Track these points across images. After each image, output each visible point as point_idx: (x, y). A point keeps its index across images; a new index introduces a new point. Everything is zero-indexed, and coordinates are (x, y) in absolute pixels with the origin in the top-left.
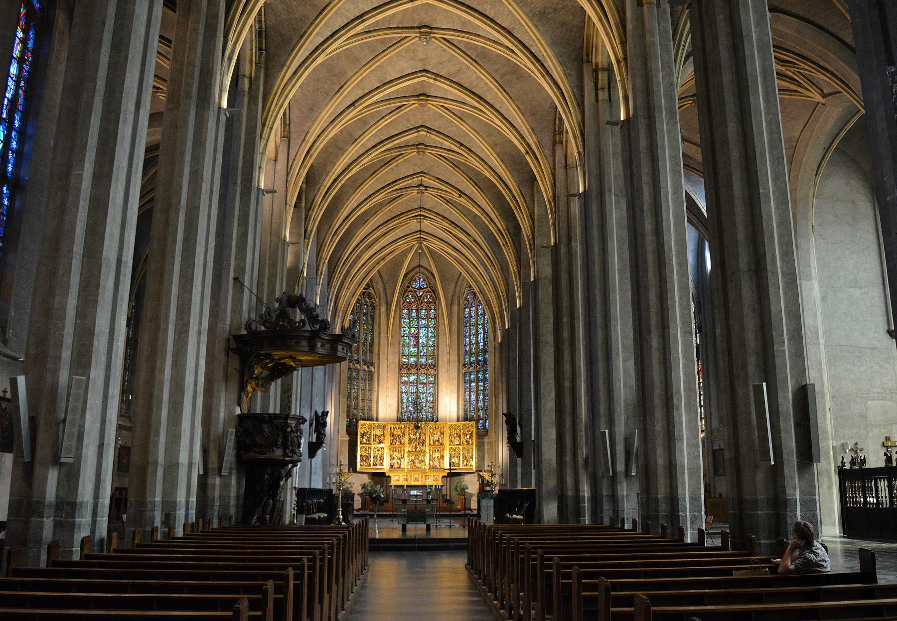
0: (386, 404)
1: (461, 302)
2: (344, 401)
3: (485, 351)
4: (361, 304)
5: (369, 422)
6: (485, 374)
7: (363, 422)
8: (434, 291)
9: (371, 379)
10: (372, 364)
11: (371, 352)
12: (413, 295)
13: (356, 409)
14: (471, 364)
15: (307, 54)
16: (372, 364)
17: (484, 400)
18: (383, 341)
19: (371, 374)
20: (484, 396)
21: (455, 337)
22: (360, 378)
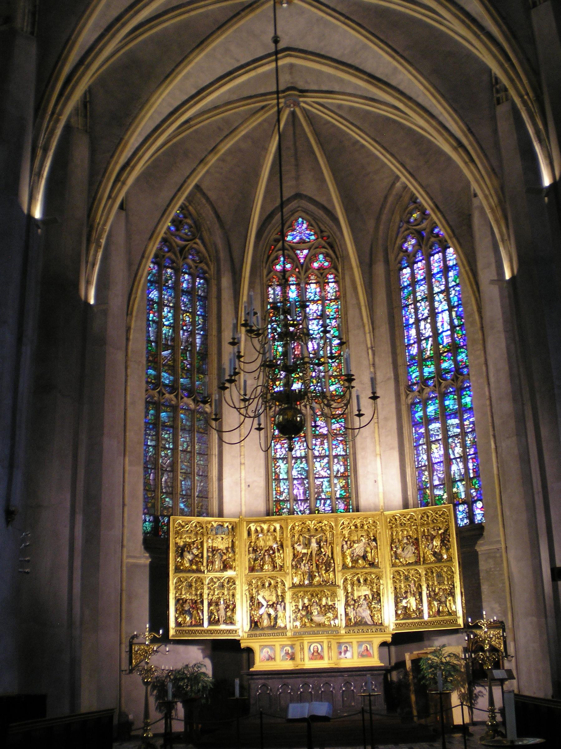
1: (392, 257)
5: (195, 520)
7: (180, 520)
15: (141, 140)
21: (384, 329)
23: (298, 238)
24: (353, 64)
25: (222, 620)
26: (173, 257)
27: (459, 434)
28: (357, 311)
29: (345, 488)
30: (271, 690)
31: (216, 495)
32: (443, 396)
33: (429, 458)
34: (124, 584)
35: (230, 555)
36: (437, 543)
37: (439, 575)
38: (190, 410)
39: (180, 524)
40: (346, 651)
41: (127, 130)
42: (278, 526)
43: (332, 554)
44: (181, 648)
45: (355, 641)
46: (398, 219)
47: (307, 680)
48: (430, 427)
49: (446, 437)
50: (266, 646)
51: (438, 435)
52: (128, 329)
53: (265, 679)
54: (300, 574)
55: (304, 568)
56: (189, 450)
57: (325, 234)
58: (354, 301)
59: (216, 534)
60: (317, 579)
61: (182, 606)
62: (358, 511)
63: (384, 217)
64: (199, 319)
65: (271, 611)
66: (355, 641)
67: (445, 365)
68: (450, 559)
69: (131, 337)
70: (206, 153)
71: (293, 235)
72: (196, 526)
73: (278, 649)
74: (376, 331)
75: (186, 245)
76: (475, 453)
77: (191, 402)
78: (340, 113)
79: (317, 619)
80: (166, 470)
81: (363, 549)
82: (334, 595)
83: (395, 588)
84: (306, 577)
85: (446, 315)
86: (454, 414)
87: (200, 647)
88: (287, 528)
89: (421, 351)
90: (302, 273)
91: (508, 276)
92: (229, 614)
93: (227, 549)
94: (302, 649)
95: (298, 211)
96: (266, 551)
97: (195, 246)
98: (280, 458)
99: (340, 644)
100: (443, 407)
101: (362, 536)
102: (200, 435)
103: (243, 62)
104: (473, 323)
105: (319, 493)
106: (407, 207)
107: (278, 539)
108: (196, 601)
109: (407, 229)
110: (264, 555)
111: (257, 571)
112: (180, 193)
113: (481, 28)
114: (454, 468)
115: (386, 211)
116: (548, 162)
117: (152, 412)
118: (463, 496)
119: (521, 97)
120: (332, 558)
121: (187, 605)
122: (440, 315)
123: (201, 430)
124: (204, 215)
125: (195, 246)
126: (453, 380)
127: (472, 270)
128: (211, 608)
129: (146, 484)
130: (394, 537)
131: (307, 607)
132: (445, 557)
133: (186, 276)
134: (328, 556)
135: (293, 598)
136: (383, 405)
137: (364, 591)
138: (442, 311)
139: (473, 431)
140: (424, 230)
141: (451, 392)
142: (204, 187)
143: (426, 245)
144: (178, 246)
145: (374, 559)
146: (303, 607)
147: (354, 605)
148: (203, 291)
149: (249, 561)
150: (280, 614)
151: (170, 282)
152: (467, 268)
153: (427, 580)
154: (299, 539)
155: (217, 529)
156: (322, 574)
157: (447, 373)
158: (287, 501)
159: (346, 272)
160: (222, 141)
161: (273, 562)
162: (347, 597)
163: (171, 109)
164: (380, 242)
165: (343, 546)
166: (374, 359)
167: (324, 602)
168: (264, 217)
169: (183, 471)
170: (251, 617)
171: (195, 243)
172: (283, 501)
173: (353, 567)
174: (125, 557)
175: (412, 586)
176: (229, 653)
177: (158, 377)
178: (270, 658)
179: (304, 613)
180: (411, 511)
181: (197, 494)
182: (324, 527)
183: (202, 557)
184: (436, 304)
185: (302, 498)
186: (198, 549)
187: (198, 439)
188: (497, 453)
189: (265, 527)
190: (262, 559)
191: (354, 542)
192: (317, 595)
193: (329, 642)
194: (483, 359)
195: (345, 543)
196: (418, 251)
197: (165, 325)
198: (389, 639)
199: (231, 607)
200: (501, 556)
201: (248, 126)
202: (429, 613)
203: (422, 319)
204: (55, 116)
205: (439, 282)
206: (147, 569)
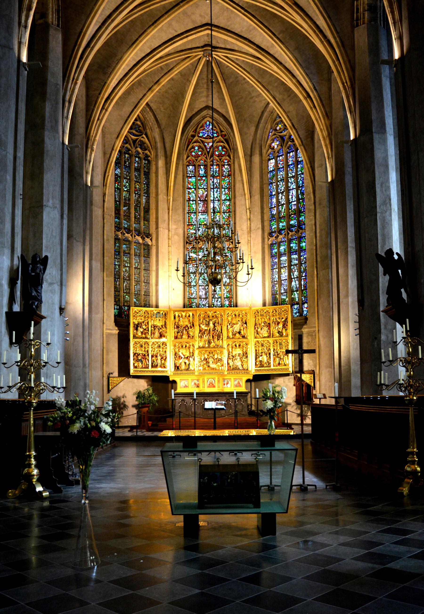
0: (168, 285)
1: (264, 151)
2: (110, 281)
3: (299, 212)
4: (131, 156)
5: (144, 309)
6: (300, 242)
7: (136, 309)
8: (228, 140)
9: (148, 255)
10: (148, 235)
11: (147, 219)
12: (199, 147)
13: (129, 293)
14: (280, 231)
16: (148, 235)
17: (299, 278)
18: (162, 205)
19: (148, 248)
20: (300, 272)
21: (257, 197)
22: (132, 252)
23: (206, 135)
24: (247, 38)
25: (159, 365)
26: (129, 147)
27: (297, 264)
28: (241, 185)
29: (230, 291)
30: (186, 403)
31: (154, 294)
32: (290, 241)
33: (279, 277)
34: (105, 344)
35: (164, 329)
36: (281, 326)
37: (281, 344)
38: (140, 243)
39: (135, 312)
40: (227, 383)
41: (109, 77)
42: (191, 314)
43: (221, 330)
44: (135, 380)
45: (232, 378)
46: (269, 127)
47: (206, 398)
48: (281, 259)
49: (290, 265)
50: (184, 380)
51: (285, 264)
52: (104, 195)
53: (183, 397)
55: (206, 337)
56: (139, 267)
57: (223, 133)
58: (241, 190)
59: (156, 317)
61: (137, 357)
62: (236, 306)
63: (261, 125)
64: (145, 187)
65: (186, 361)
66: (232, 378)
67: (292, 222)
68: (287, 336)
69: (106, 200)
70: (153, 84)
71: (203, 133)
72: (145, 313)
73: (190, 381)
74: (252, 198)
75: (137, 139)
76: (306, 276)
77: (140, 239)
78: (237, 62)
79: (212, 365)
80: (126, 279)
81: (239, 328)
82: (221, 353)
83: (256, 350)
84: (207, 343)
85: (294, 192)
86: (296, 252)
87: (146, 380)
88: (196, 315)
89: (279, 212)
90: (208, 158)
91: (330, 179)
92: (163, 362)
93: (162, 326)
94: (204, 382)
95: (207, 117)
96: (184, 327)
97: (142, 139)
98: (192, 273)
99: (224, 380)
100: (290, 248)
101: (239, 321)
102: (145, 258)
103: (180, 32)
104: (309, 199)
105: (214, 295)
106: (275, 120)
107: (191, 321)
108: (145, 355)
109: (275, 134)
110: (183, 330)
111: (179, 339)
112: (136, 110)
113: (325, 37)
114: (293, 283)
115: (262, 121)
116: (353, 125)
117: (117, 245)
118: (297, 300)
119: (343, 84)
120: (221, 332)
121: (140, 356)
122: (291, 191)
123: (146, 256)
124: (148, 119)
125: (142, 139)
126: (296, 232)
127: (311, 167)
128: (153, 358)
129: (115, 287)
130: (257, 322)
131: (206, 359)
132: (284, 334)
133: (137, 159)
135: (199, 354)
136: (254, 244)
137: (238, 351)
138: (292, 189)
139: (305, 263)
140: (285, 136)
141: (294, 239)
142: (151, 105)
143: (286, 146)
144: (132, 139)
145: (245, 334)
146: (204, 359)
147: (233, 359)
148: (147, 169)
149: (175, 333)
150: (191, 362)
151: (127, 163)
152: (309, 166)
153: (273, 346)
154: (203, 321)
155: (157, 314)
157: (293, 227)
158: (196, 298)
159: (235, 159)
160: (162, 77)
161: (188, 333)
162: (229, 354)
163: (135, 63)
164: (258, 141)
165: (227, 326)
166: (250, 215)
167: (216, 357)
168: (186, 121)
169: (136, 280)
170: (175, 364)
171: (143, 137)
172: (193, 298)
173: (233, 338)
174: (105, 329)
175: (265, 349)
176: (162, 383)
177: (120, 223)
178: (186, 386)
179: (205, 362)
180: (267, 308)
181: (143, 293)
182: (217, 315)
183: (148, 330)
184: (289, 184)
185: (204, 297)
186: (146, 325)
187: (144, 261)
188: (317, 277)
189: (184, 314)
190: (182, 332)
191: (234, 324)
192: (212, 353)
193: (218, 378)
194: (313, 222)
195: (228, 324)
196: (280, 149)
197: (124, 191)
198: (251, 378)
199: (164, 358)
200: (315, 335)
201: (179, 68)
202: (274, 364)
203: (280, 193)
204: (75, 80)
205: (292, 170)
206: (117, 336)
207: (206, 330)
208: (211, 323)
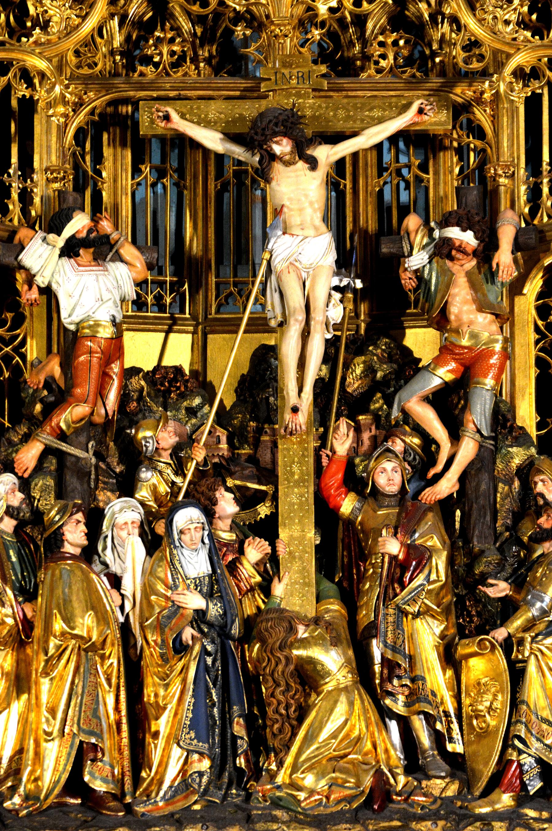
54: (89, 649)
55: (148, 561)
60: (339, 715)
84: (172, 697)
134: (502, 418)
154: (84, 183)
156: (399, 664)
207: (166, 385)
208: (298, 190)
